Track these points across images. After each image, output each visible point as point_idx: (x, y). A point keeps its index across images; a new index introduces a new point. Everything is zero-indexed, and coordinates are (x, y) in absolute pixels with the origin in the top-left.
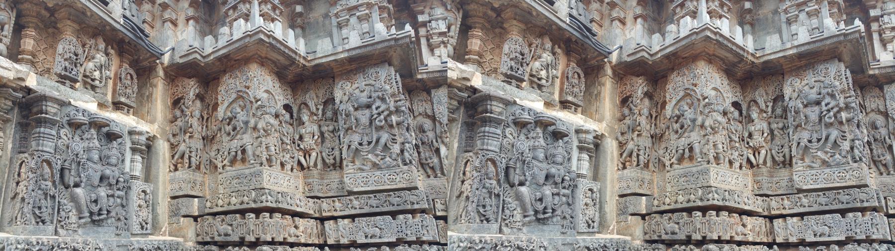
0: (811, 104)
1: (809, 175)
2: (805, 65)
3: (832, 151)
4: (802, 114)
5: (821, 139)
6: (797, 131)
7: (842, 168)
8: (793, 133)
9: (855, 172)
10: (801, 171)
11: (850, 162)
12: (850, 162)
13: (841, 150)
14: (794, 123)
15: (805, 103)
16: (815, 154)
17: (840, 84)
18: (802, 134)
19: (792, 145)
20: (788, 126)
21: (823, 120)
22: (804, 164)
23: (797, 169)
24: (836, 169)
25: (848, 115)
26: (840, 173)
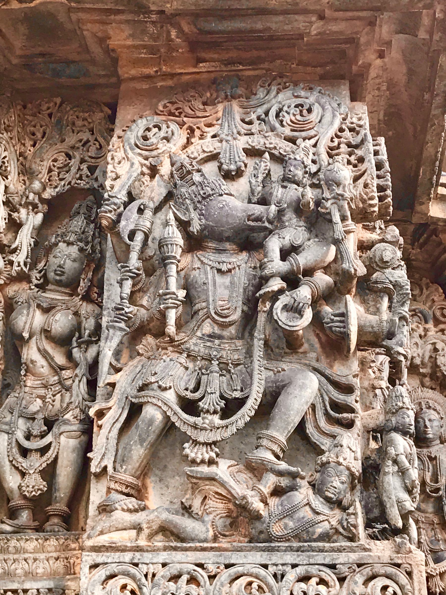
0: (220, 239)
1: (161, 572)
2: (214, 82)
3: (283, 466)
4: (173, 270)
5: (241, 402)
6: (136, 354)
7: (320, 558)
8: (117, 354)
9: (380, 582)
10: (123, 550)
11: (361, 532)
12: (361, 532)
13: (324, 465)
14: (130, 309)
15: (195, 227)
16: (204, 469)
17: (356, 179)
18: (159, 367)
19: (101, 414)
20: (98, 328)
21: (262, 318)
22: (140, 517)
23: (104, 540)
24: (290, 558)
25: (372, 319)
26: (305, 579)
